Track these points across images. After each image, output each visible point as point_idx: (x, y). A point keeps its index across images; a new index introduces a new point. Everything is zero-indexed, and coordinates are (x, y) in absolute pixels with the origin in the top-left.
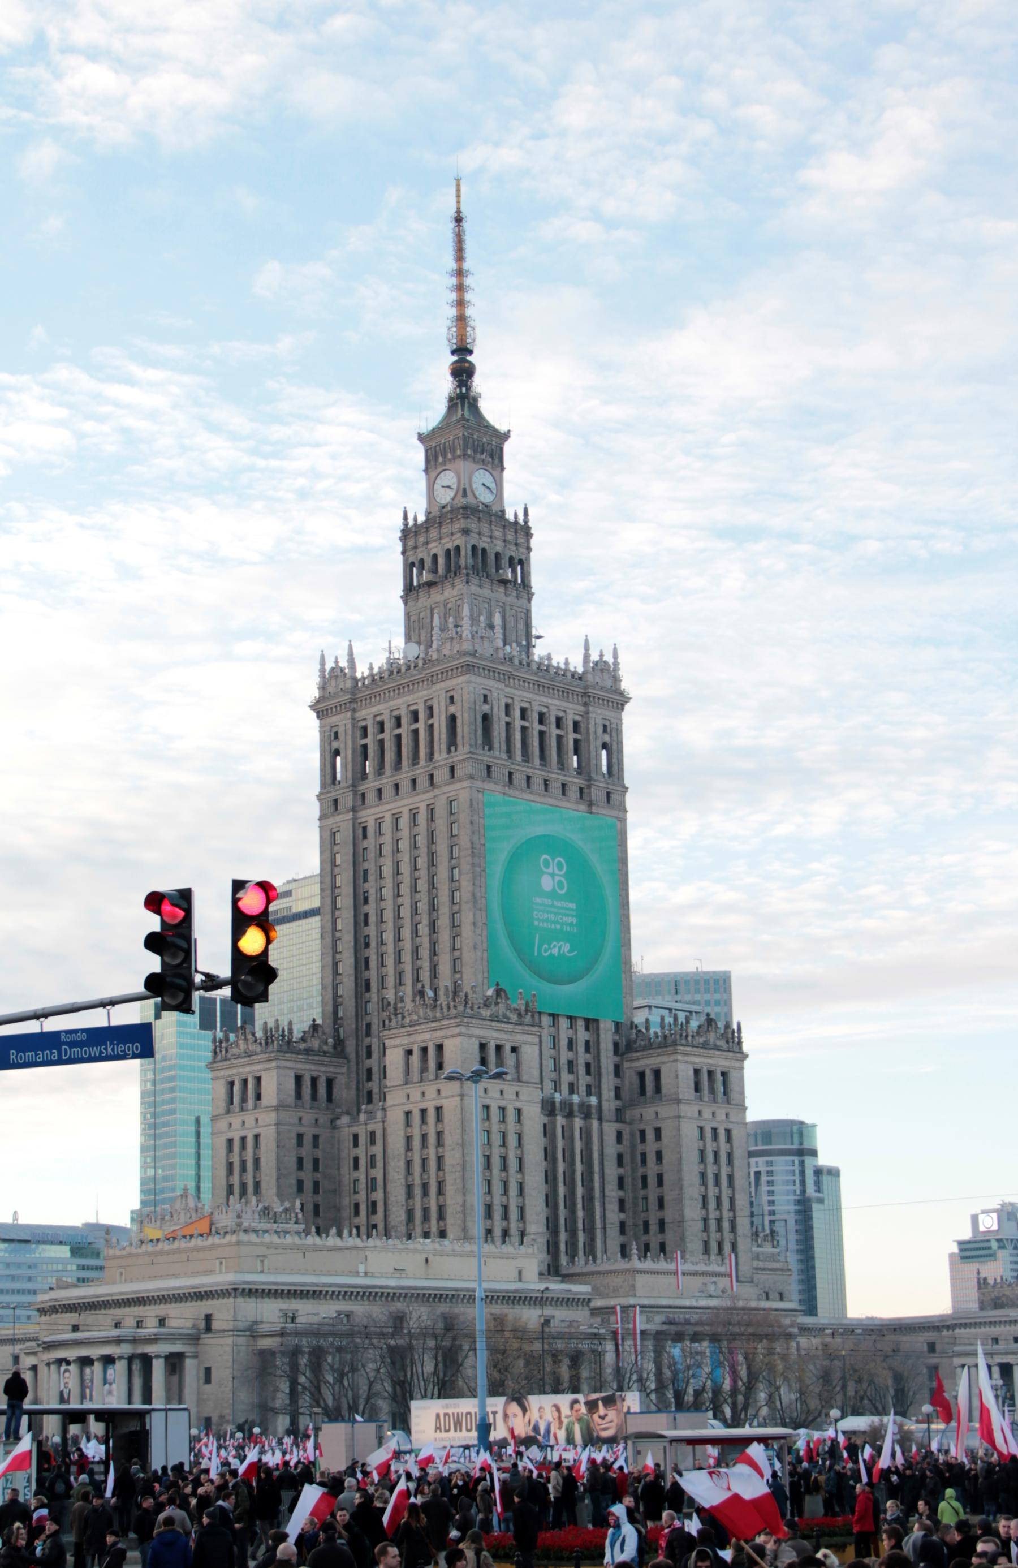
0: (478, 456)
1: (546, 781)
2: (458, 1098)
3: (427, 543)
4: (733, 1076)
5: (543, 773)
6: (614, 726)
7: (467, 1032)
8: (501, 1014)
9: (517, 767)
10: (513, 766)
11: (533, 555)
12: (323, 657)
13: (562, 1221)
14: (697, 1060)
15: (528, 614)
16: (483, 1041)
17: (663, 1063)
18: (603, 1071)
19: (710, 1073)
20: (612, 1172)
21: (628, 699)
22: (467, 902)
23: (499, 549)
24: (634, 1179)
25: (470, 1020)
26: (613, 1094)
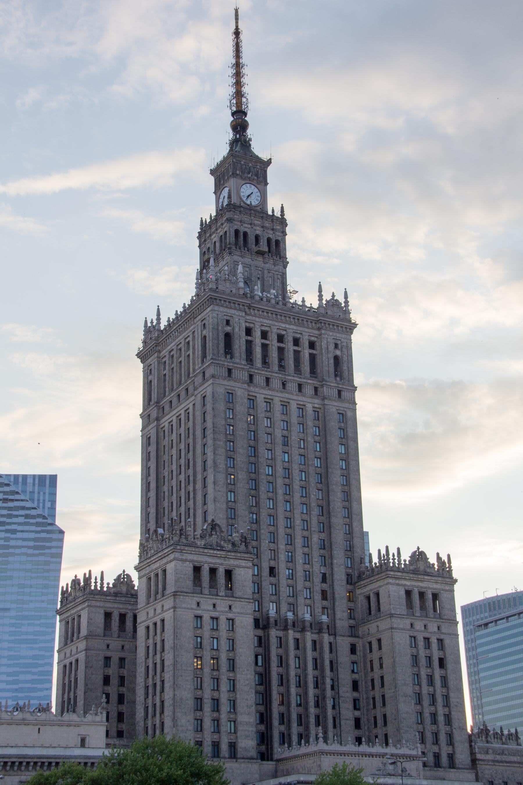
0: (246, 175)
1: (283, 383)
2: (172, 610)
3: (210, 235)
4: (444, 596)
5: (280, 376)
6: (345, 344)
7: (180, 557)
8: (214, 542)
9: (256, 371)
10: (253, 370)
11: (289, 239)
12: (146, 322)
13: (294, 716)
14: (408, 583)
15: (284, 276)
16: (197, 564)
17: (380, 587)
18: (337, 596)
19: (422, 595)
20: (345, 678)
21: (355, 325)
22: (210, 468)
23: (258, 232)
24: (366, 682)
25: (182, 547)
26: (346, 615)
